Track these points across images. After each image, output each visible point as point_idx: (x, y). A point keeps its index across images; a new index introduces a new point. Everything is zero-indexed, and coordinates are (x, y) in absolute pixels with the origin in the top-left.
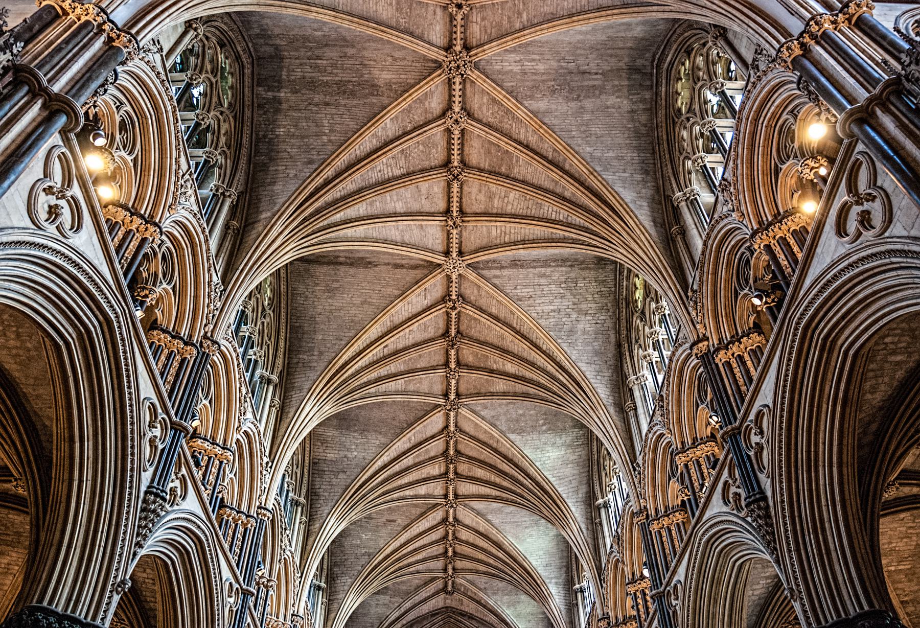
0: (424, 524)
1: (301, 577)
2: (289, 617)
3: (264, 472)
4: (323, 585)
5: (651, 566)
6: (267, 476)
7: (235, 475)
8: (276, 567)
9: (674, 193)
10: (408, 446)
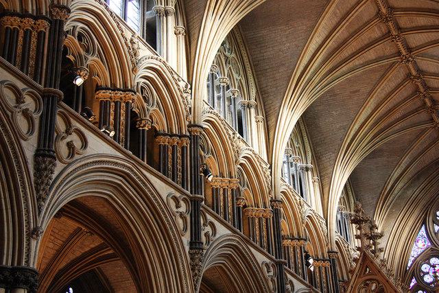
2: (268, 203)
3: (185, 95)
4: (310, 165)
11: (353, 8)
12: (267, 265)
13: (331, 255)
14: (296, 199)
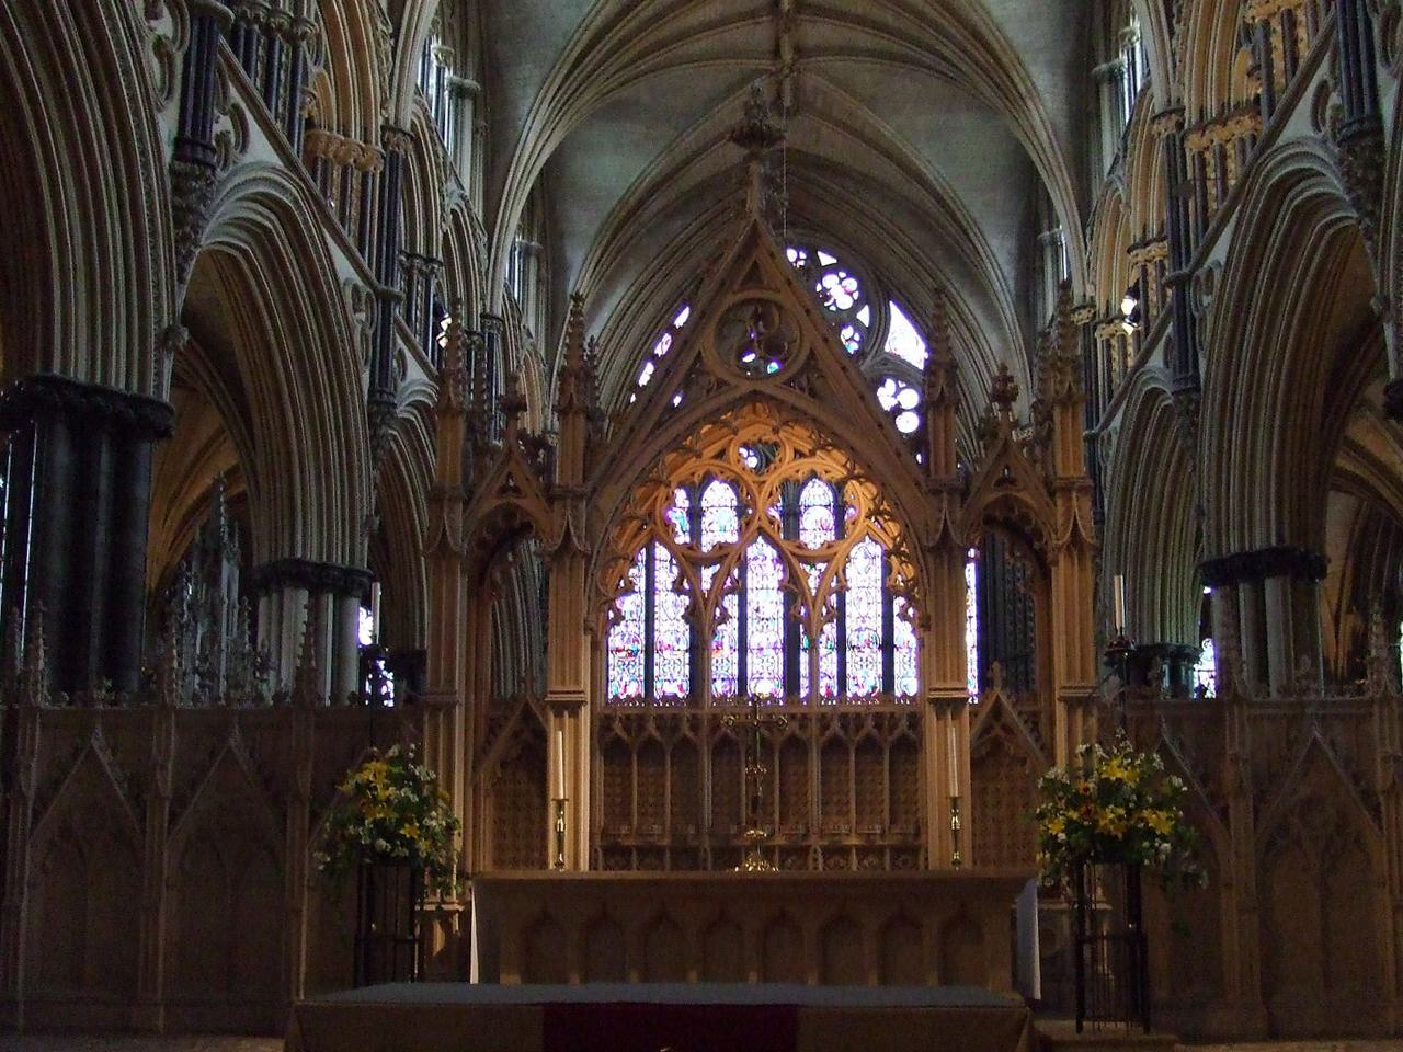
2: (375, 133)
4: (470, 82)
12: (356, 289)
13: (488, 322)
14: (436, 153)
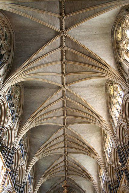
0: (60, 161)
1: (26, 172)
3: (15, 139)
5: (121, 161)
6: (16, 140)
7: (7, 138)
8: (19, 167)
9: (119, 59)
10: (54, 138)
11: (59, 137)
